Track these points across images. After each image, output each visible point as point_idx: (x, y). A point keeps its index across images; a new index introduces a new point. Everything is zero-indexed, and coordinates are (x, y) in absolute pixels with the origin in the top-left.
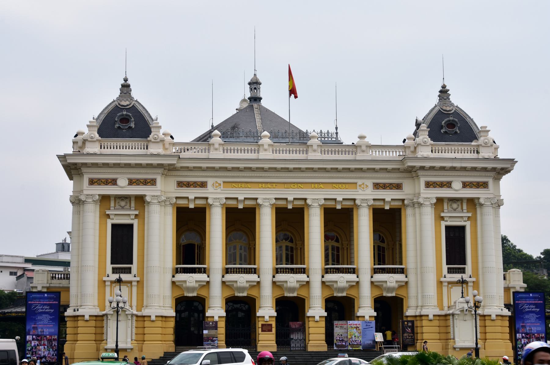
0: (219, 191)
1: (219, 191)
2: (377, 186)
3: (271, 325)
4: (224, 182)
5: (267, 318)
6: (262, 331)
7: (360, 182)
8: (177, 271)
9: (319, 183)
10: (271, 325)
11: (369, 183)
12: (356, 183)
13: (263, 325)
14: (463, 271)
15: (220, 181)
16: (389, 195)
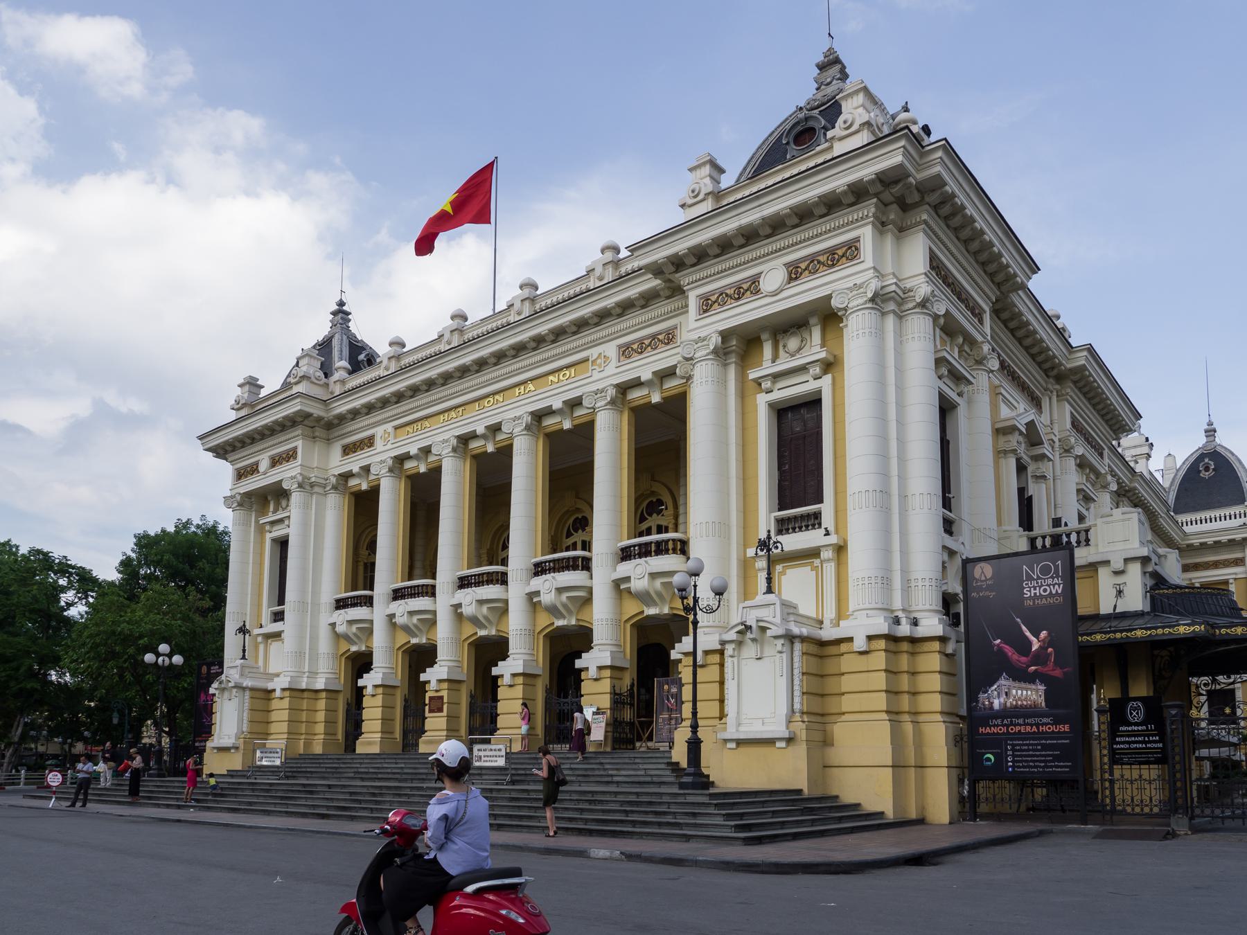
0: (389, 446)
1: (389, 446)
2: (626, 351)
3: (442, 698)
4: (396, 428)
5: (433, 685)
6: (430, 711)
7: (593, 353)
8: (341, 604)
9: (524, 382)
10: (442, 698)
11: (611, 349)
12: (586, 360)
13: (431, 698)
14: (814, 520)
15: (389, 427)
16: (644, 367)
